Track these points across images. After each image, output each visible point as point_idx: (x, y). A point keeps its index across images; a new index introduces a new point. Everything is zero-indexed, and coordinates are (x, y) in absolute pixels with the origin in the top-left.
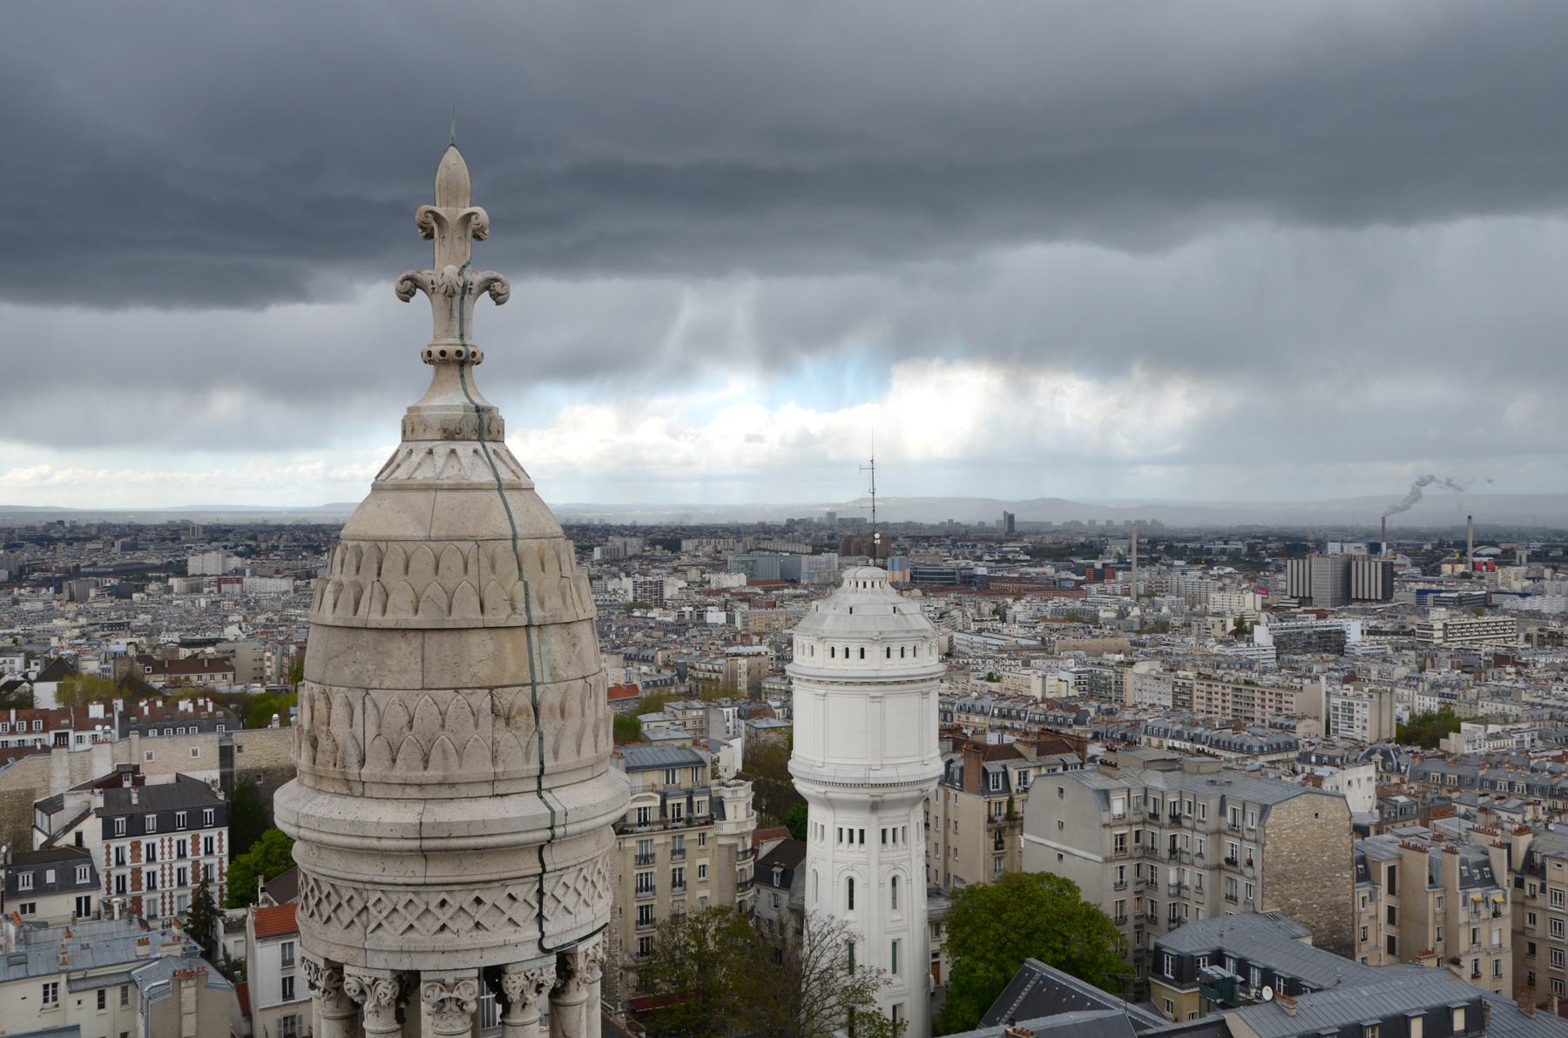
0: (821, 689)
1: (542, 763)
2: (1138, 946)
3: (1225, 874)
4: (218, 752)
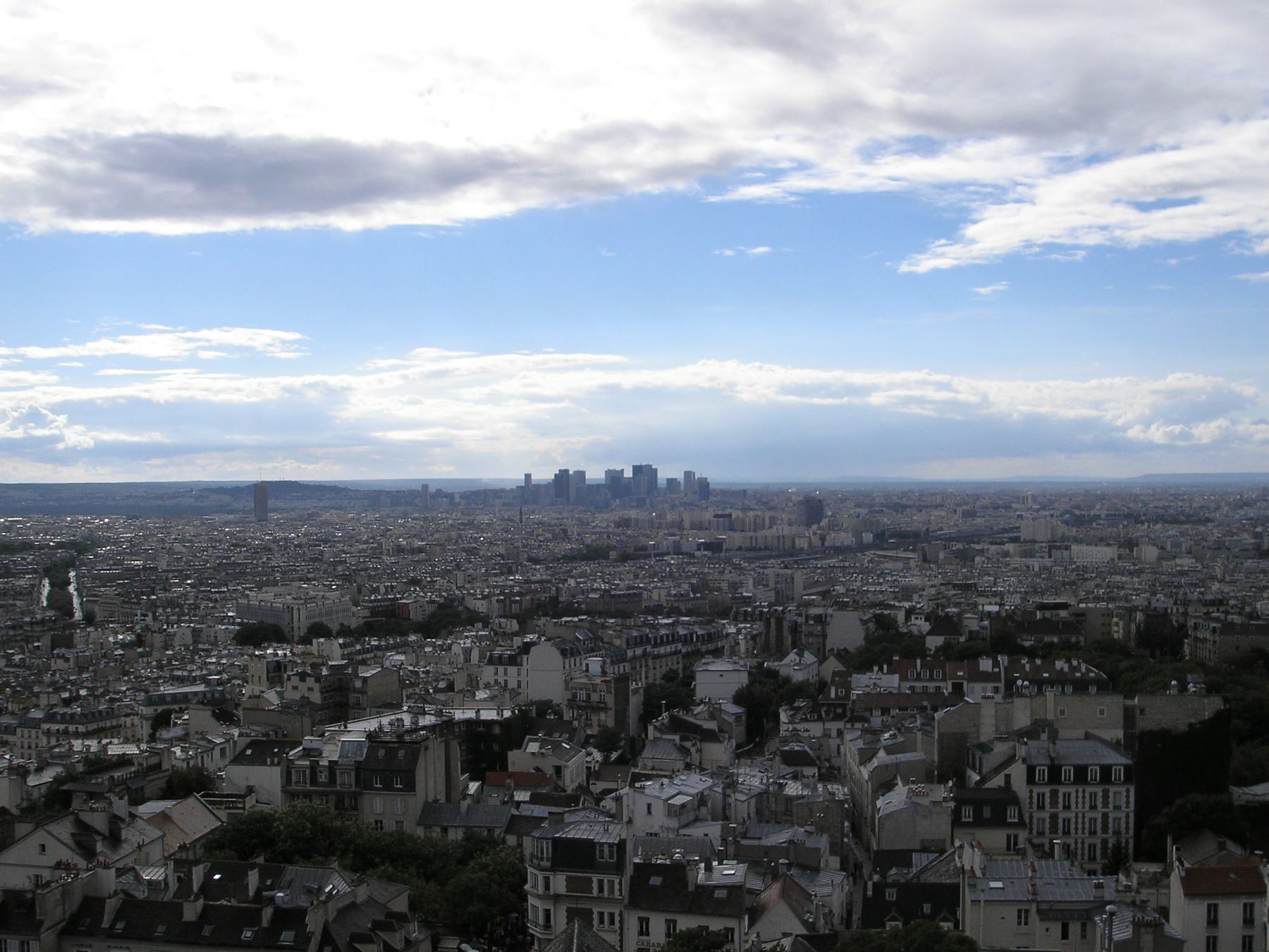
4: (1122, 713)
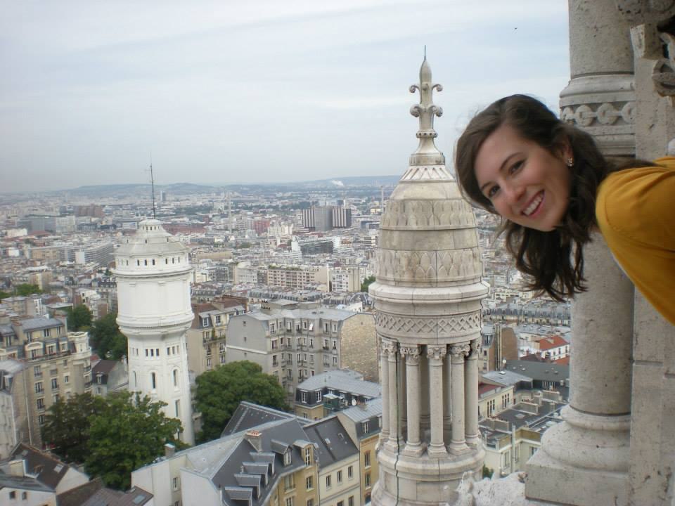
3: (323, 354)
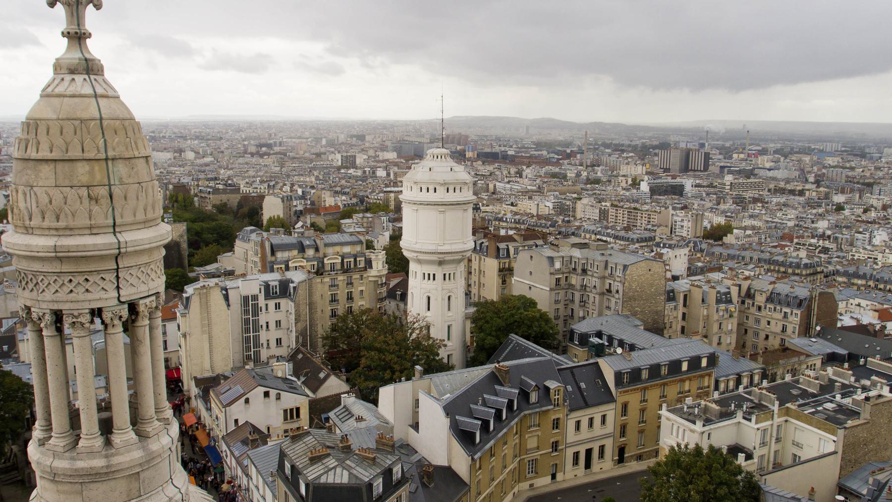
0: (415, 207)
1: (114, 220)
2: (565, 329)
3: (605, 297)
